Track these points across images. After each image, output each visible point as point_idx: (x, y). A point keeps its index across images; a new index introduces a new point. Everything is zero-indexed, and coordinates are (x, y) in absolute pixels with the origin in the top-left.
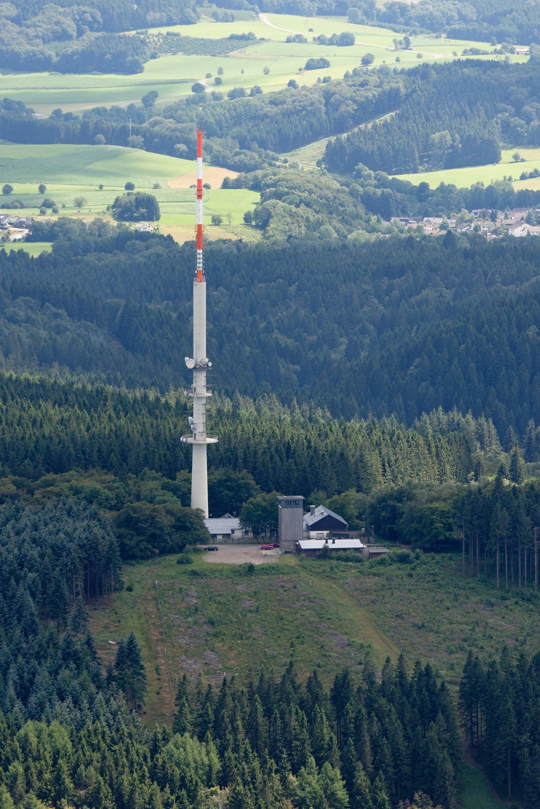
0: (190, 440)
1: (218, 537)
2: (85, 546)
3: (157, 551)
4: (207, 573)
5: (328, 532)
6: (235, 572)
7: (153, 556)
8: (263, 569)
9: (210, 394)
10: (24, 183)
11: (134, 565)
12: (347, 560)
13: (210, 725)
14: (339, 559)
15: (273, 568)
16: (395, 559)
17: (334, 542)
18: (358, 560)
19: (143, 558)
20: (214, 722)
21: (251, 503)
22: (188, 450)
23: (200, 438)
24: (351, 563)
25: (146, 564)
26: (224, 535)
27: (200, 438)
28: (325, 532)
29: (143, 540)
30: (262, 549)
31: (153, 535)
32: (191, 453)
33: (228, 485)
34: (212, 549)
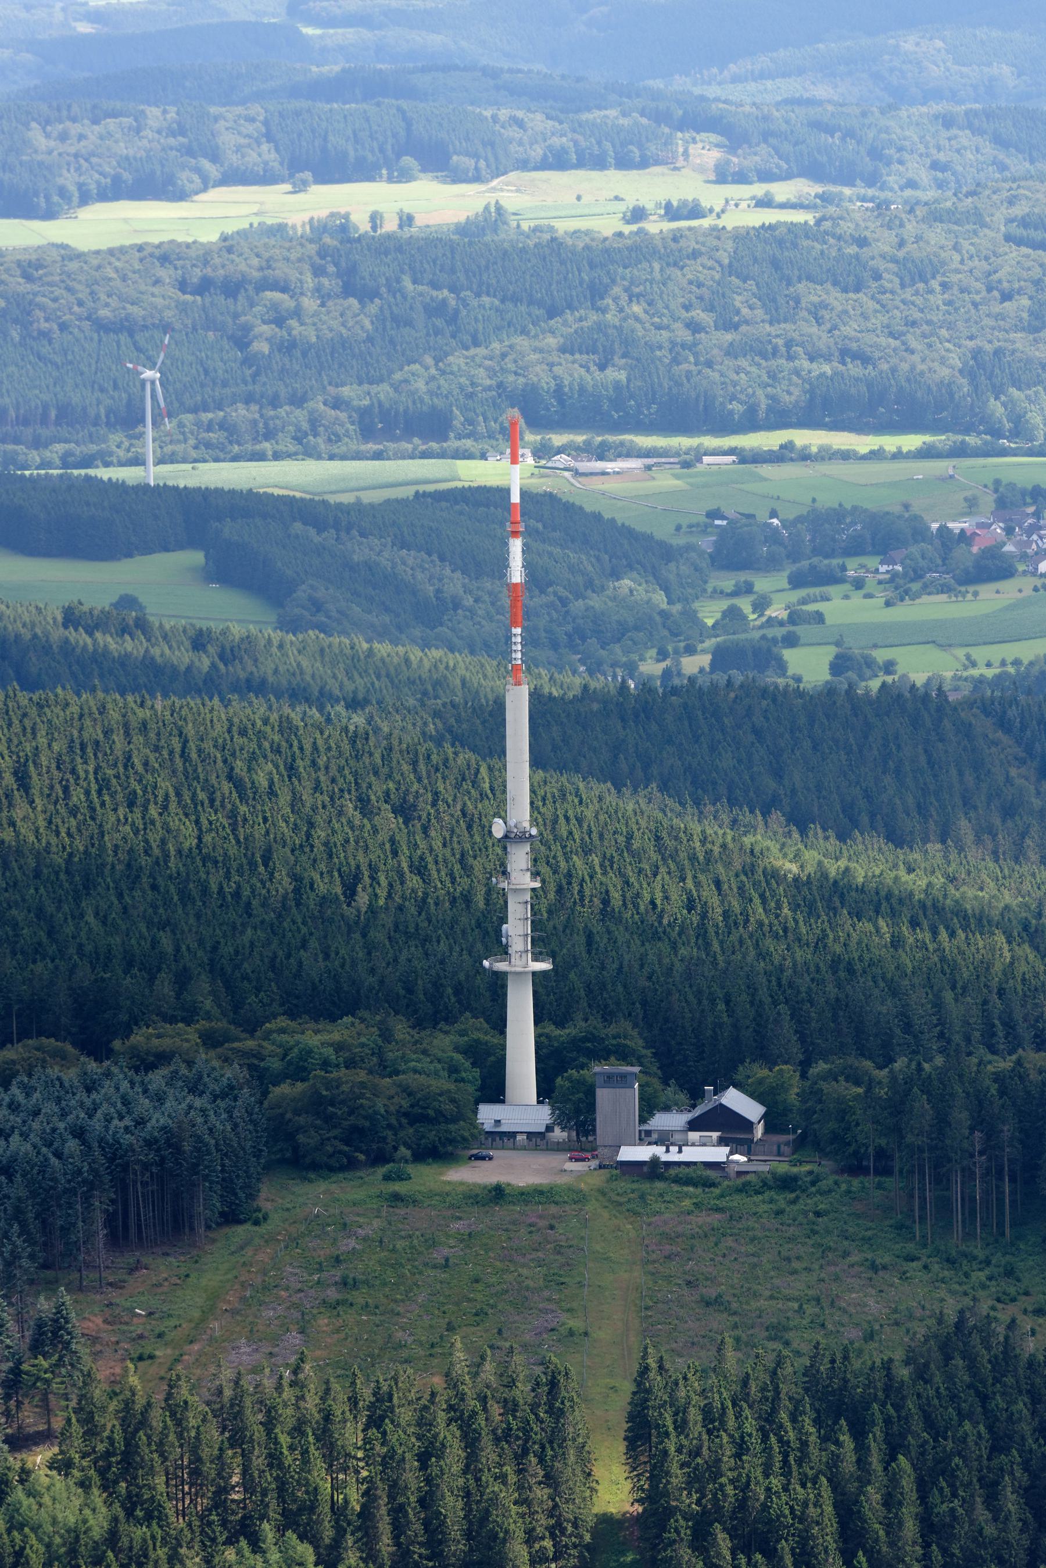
0: (501, 966)
1: (519, 1138)
2: (156, 1141)
3: (362, 1157)
4: (420, 1197)
5: (718, 1134)
6: (470, 1197)
7: (351, 1165)
8: (522, 1194)
9: (537, 885)
10: (388, 502)
11: (310, 1181)
12: (689, 1181)
13: (113, 1459)
14: (677, 1180)
15: (541, 1193)
16: (771, 1183)
17: (680, 1151)
18: (710, 1184)
19: (332, 1169)
20: (123, 1453)
21: (569, 1079)
22: (498, 984)
23: (518, 963)
24: (691, 1189)
25: (334, 1179)
26: (530, 1135)
27: (518, 963)
28: (715, 1135)
29: (335, 1138)
30: (571, 1159)
31: (356, 1130)
32: (504, 987)
33: (588, 1048)
34: (483, 1158)
